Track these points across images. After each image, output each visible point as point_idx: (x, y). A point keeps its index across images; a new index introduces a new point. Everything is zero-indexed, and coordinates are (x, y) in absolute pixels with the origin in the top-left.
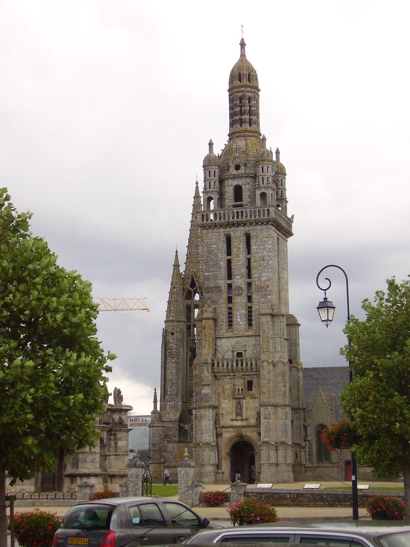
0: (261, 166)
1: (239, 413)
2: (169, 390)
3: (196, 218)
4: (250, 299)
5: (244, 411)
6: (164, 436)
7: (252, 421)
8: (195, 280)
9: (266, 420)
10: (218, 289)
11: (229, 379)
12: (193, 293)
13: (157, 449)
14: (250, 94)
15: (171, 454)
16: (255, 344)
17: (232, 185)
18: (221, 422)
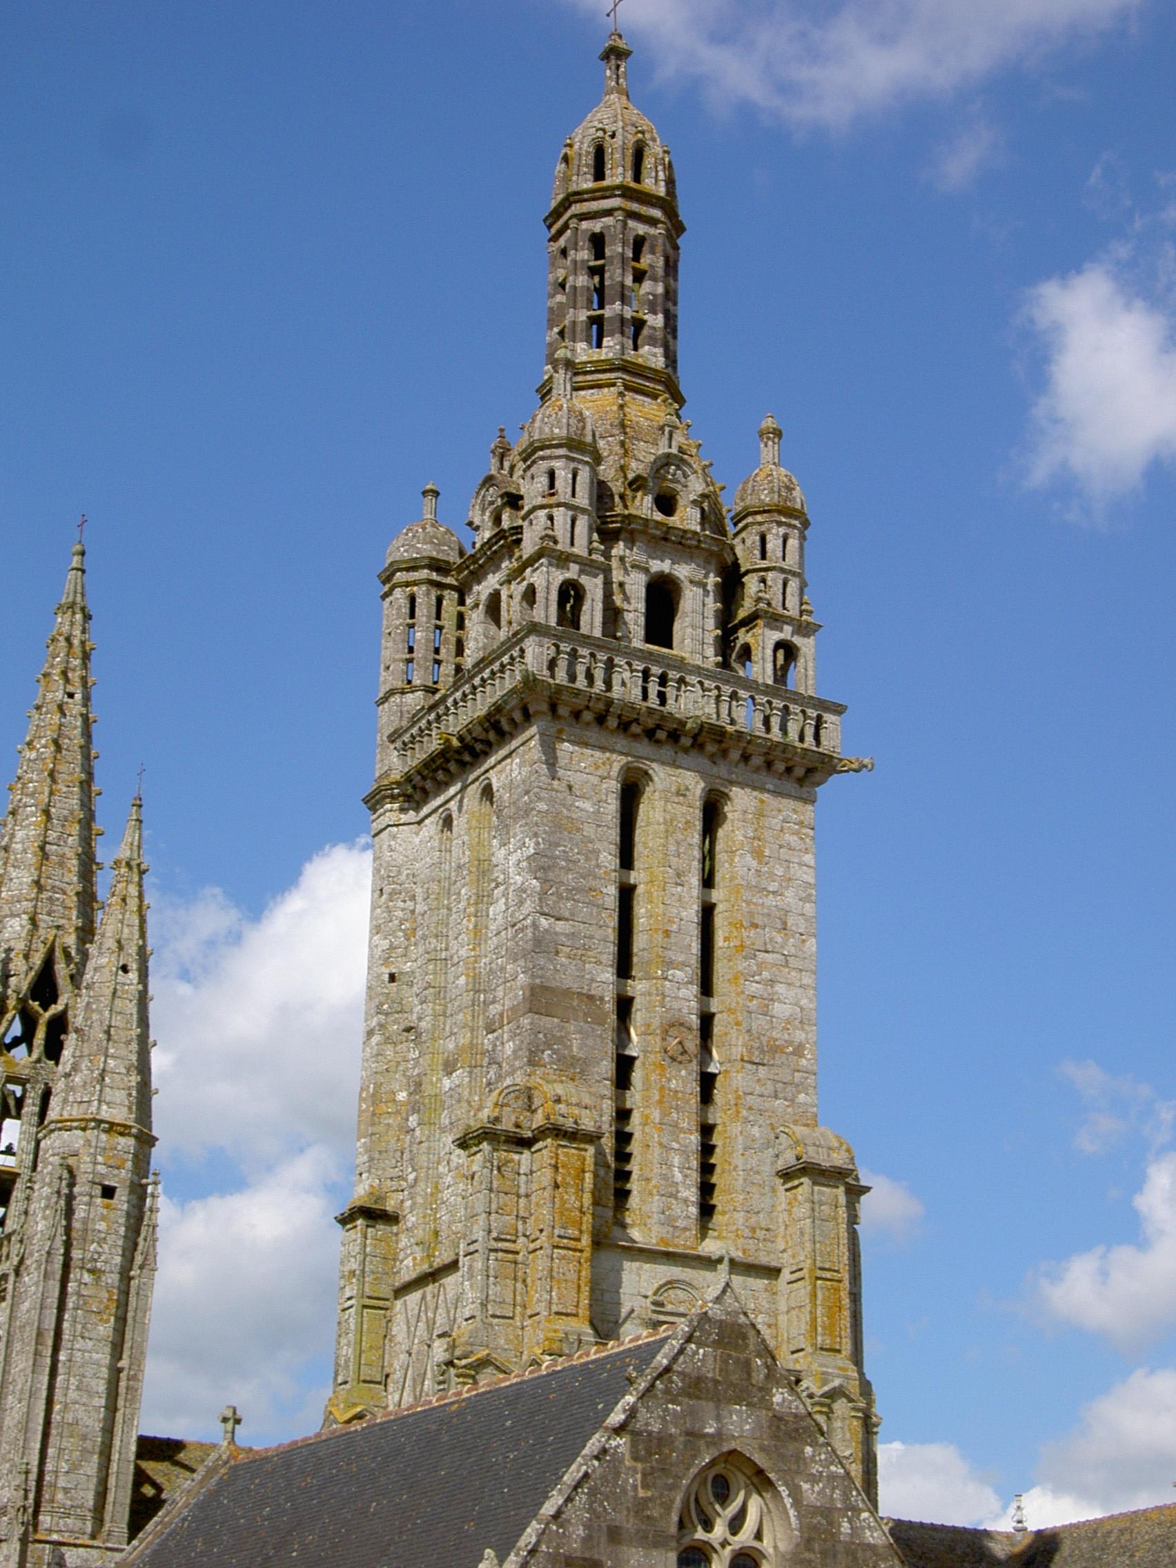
0: (782, 530)
2: (62, 1483)
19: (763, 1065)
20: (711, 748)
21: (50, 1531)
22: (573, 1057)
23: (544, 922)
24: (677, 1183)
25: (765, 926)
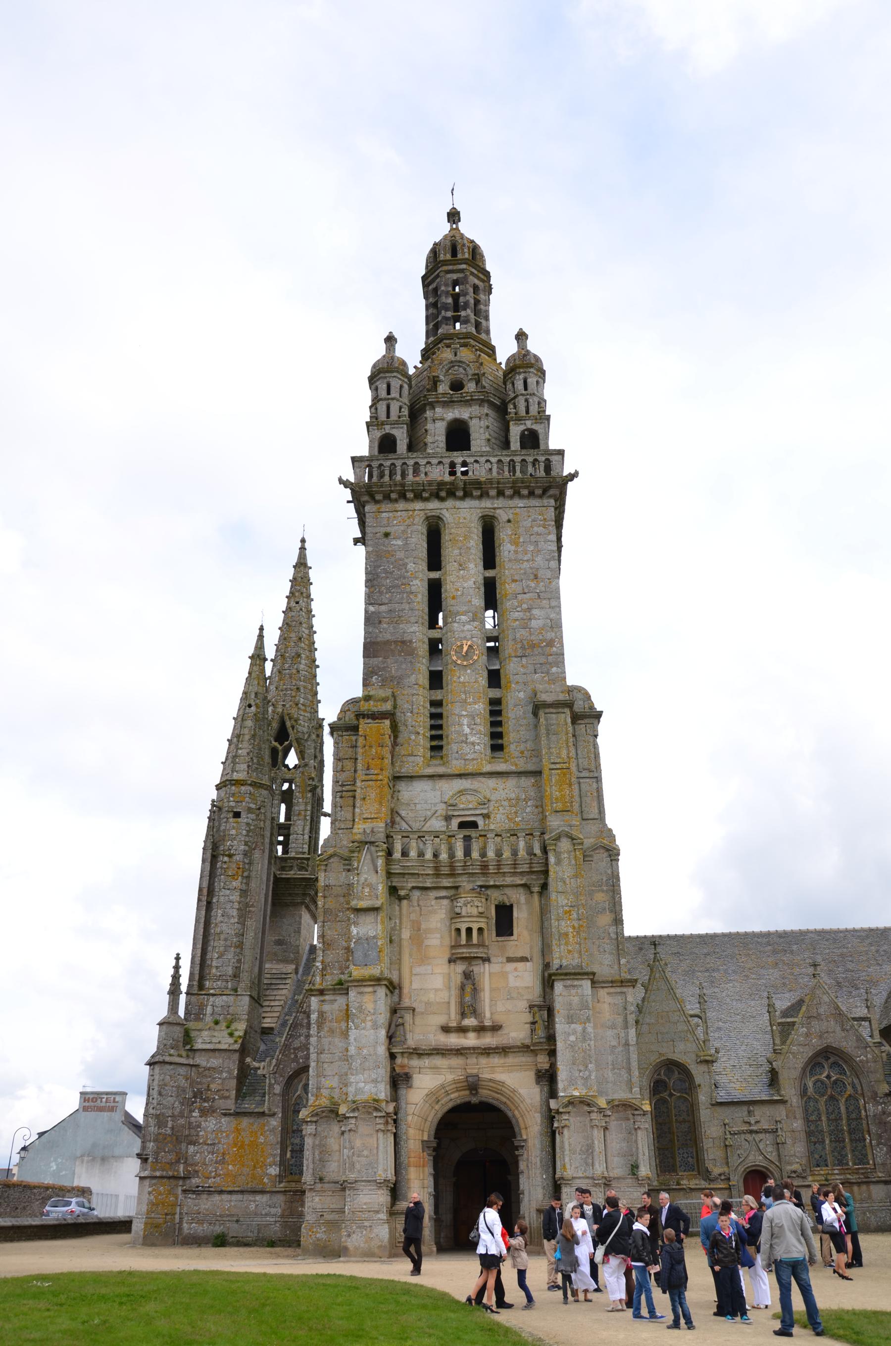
0: (522, 376)
1: (469, 1007)
2: (214, 964)
3: (297, 603)
4: (494, 678)
5: (487, 1001)
6: (191, 1094)
7: (513, 1034)
8: (288, 724)
9: (573, 1026)
10: (404, 646)
11: (437, 898)
12: (280, 754)
13: (169, 1132)
14: (477, 282)
15: (210, 1148)
16: (518, 799)
17: (443, 419)
18: (409, 1036)
19: (526, 656)
20: (476, 493)
21: (209, 989)
22: (392, 677)
23: (372, 609)
24: (466, 734)
25: (522, 580)
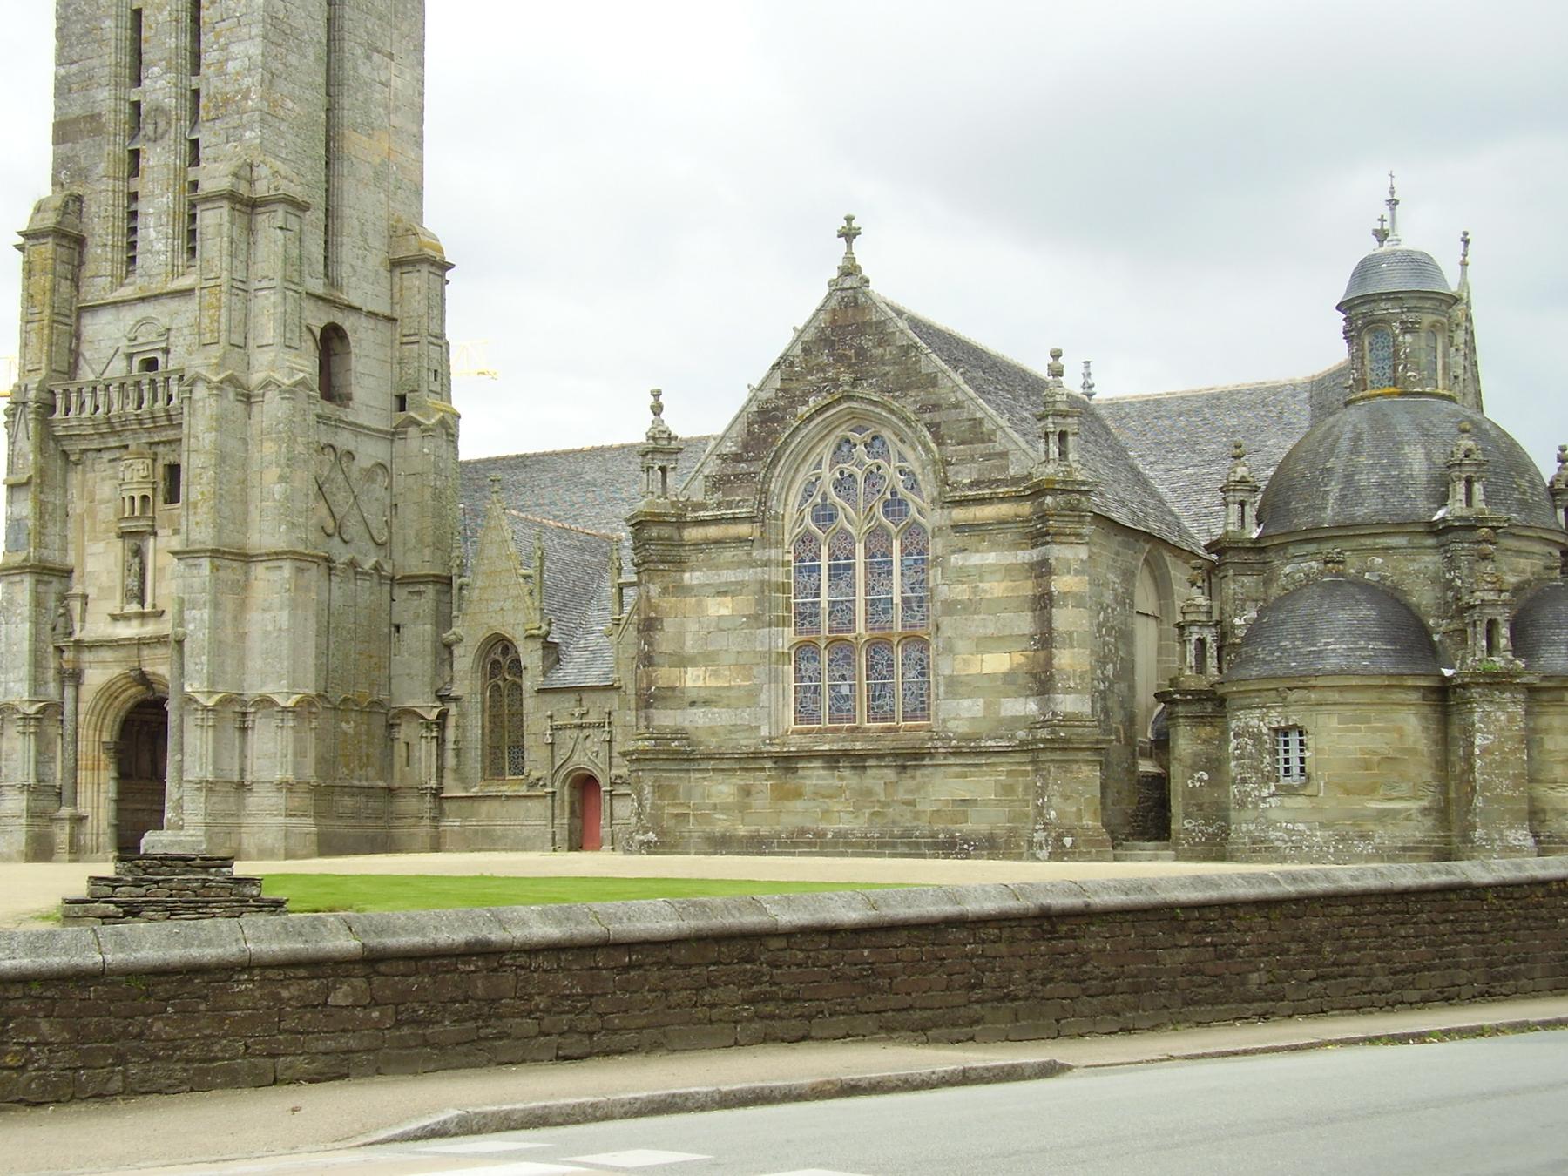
11: (110, 461)
